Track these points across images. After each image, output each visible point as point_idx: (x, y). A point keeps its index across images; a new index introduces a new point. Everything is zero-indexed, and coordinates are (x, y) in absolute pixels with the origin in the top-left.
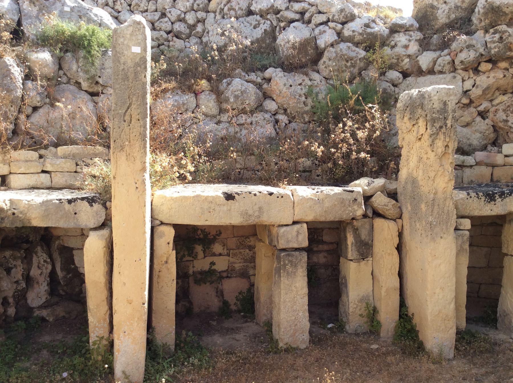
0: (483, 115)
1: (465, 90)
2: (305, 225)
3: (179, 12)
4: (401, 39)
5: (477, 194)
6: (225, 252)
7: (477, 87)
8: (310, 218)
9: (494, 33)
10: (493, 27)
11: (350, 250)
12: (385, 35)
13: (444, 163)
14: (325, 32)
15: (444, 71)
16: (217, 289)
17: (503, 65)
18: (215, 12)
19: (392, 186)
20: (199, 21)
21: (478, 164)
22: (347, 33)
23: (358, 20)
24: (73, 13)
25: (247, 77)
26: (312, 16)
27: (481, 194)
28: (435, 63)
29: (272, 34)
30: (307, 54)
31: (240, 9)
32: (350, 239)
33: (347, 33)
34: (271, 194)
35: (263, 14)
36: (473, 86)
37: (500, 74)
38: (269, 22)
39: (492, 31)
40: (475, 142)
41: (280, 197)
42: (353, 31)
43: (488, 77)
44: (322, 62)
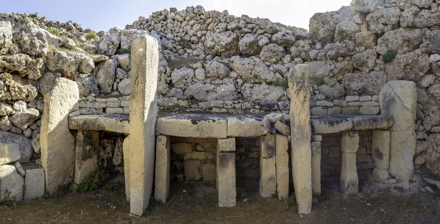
3: (194, 32)
4: (301, 43)
5: (325, 122)
6: (203, 150)
9: (343, 43)
11: (263, 152)
13: (305, 106)
14: (262, 38)
17: (348, 58)
18: (210, 30)
19: (287, 117)
20: (203, 35)
22: (274, 38)
23: (279, 32)
25: (221, 61)
26: (257, 30)
27: (327, 122)
29: (237, 39)
31: (222, 28)
32: (263, 146)
35: (233, 30)
37: (346, 63)
38: (235, 34)
42: (277, 38)
44: (261, 53)
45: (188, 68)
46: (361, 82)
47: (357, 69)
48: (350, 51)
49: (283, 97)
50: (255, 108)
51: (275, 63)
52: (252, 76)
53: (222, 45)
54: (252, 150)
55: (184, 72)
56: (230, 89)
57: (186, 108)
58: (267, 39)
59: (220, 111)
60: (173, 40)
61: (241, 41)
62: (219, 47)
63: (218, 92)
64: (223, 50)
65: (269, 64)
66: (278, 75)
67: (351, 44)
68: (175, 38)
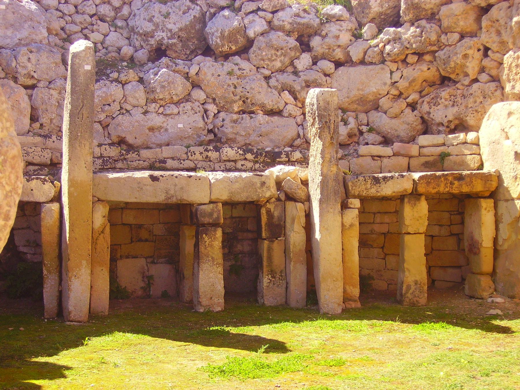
0: (413, 106)
1: (393, 81)
2: (220, 205)
4: (332, 28)
7: (404, 79)
8: (225, 197)
10: (418, 21)
11: (263, 230)
12: (316, 26)
15: (374, 62)
16: (143, 274)
17: (428, 58)
20: (125, 3)
21: (394, 155)
24: (8, 11)
28: (365, 53)
30: (236, 42)
33: (276, 22)
34: (190, 177)
36: (401, 77)
38: (198, 8)
39: (416, 24)
40: (402, 134)
41: (198, 179)
42: (283, 21)
43: (414, 69)
44: (252, 50)
45: (112, 82)
46: (453, 105)
47: (449, 79)
48: (431, 45)
49: (296, 139)
50: (246, 159)
51: (282, 71)
52: (238, 97)
53: (171, 31)
54: (239, 238)
55: (104, 89)
56: (194, 124)
57: (115, 161)
58: (264, 23)
59: (181, 166)
60: (57, 10)
61: (210, 24)
62: (164, 35)
63: (170, 131)
64: (174, 41)
65: (267, 73)
66: (286, 95)
67: (432, 32)
68: (62, 7)
